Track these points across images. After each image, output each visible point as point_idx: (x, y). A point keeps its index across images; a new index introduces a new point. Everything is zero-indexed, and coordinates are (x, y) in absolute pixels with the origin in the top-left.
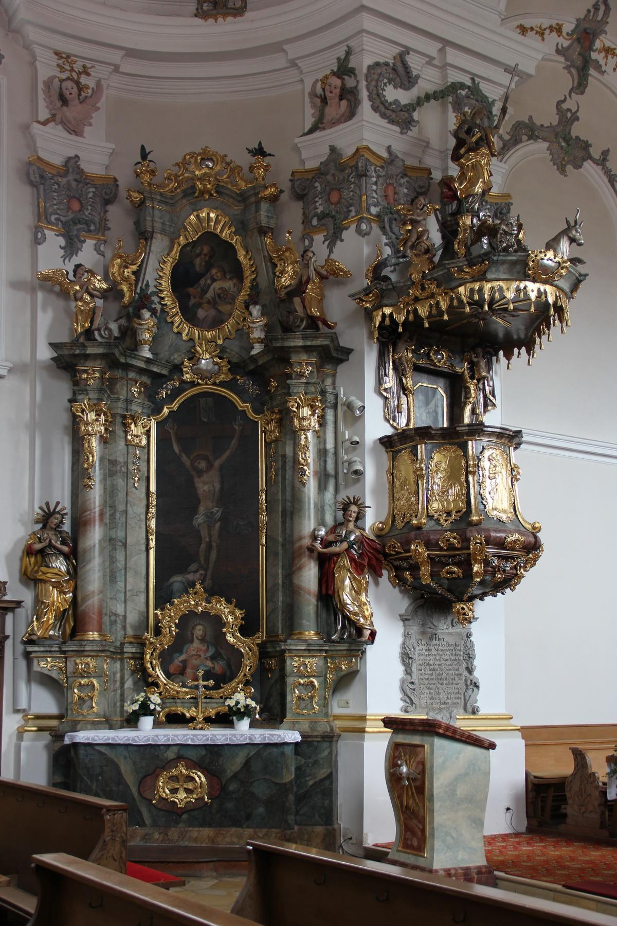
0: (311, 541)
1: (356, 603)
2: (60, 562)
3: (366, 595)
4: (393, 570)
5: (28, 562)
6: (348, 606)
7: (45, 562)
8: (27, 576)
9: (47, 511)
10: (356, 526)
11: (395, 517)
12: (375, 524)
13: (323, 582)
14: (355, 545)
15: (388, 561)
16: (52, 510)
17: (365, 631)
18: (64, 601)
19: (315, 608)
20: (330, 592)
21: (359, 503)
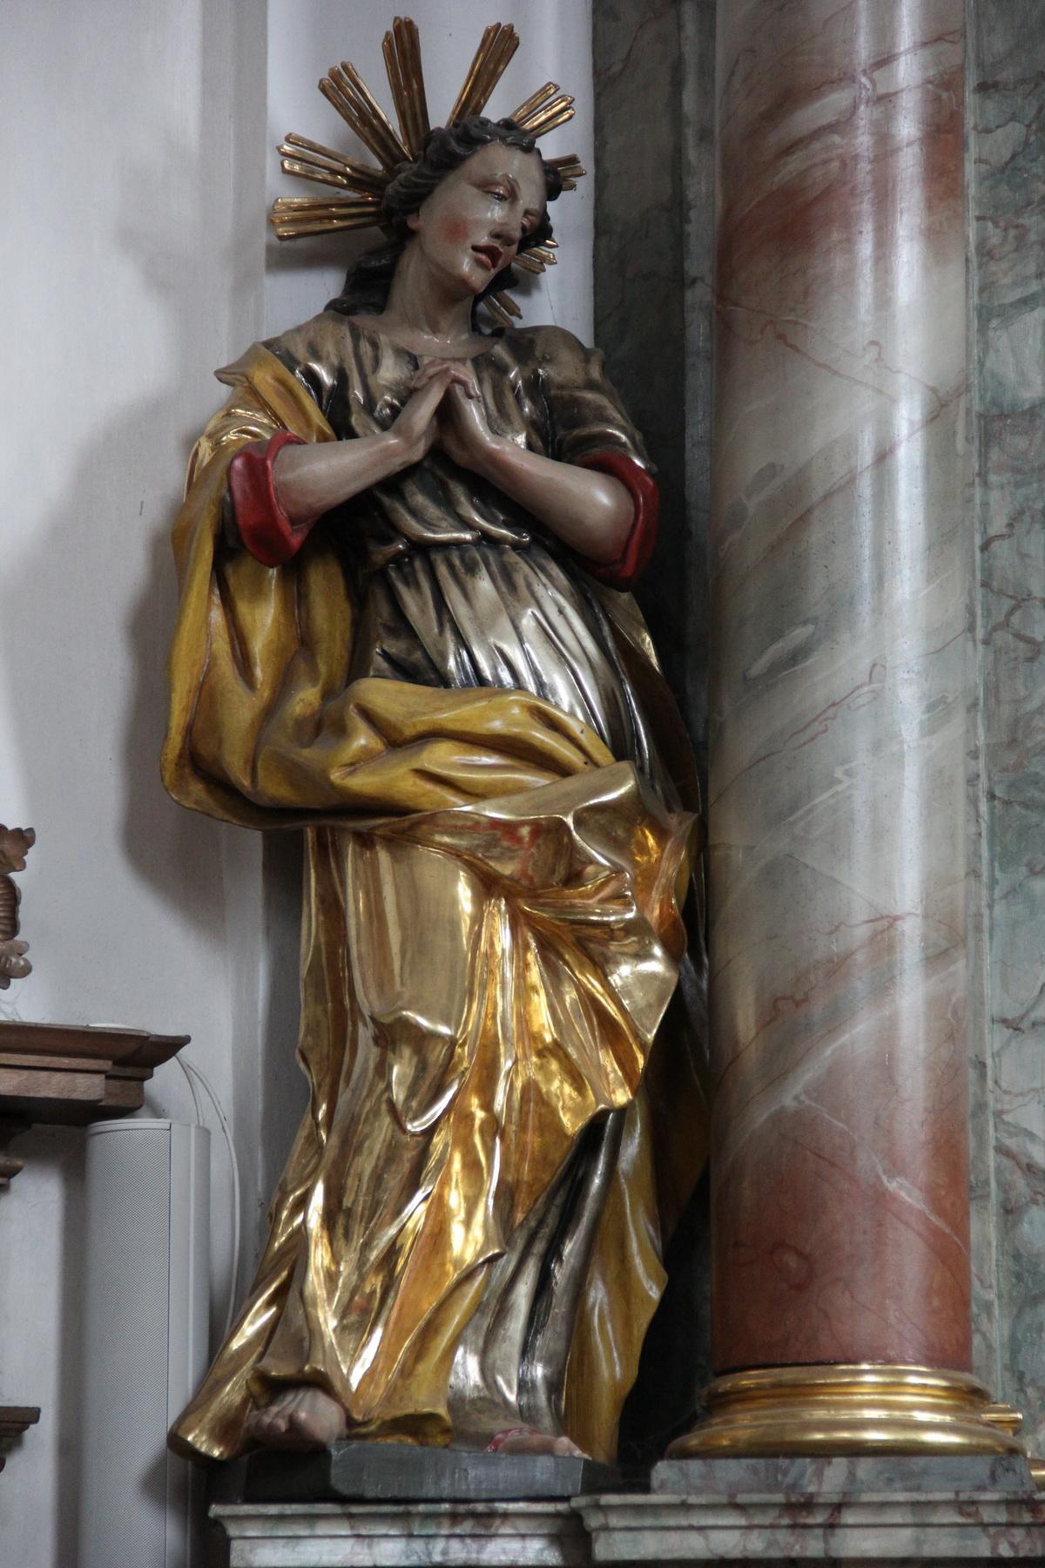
2: (549, 636)
5: (222, 646)
7: (402, 625)
8: (219, 784)
9: (388, 113)
16: (440, 114)
18: (583, 1031)
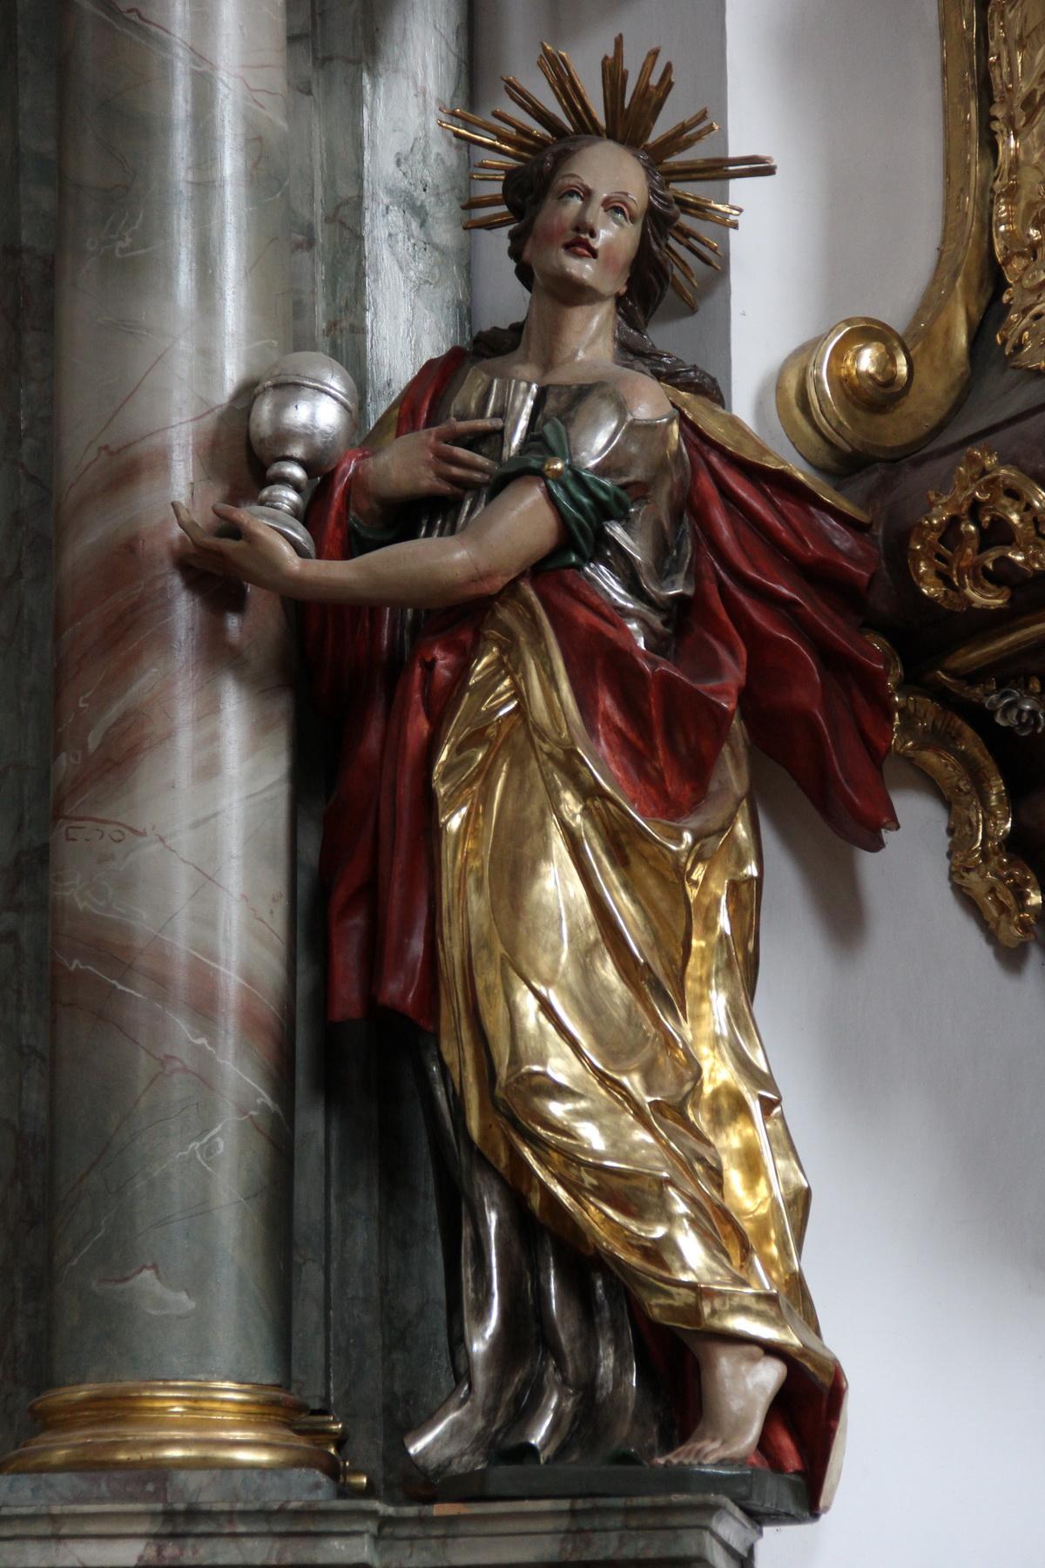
0: (215, 494)
1: (633, 1082)
3: (740, 1016)
4: (996, 788)
6: (557, 1109)
10: (632, 352)
11: (1000, 285)
12: (808, 350)
13: (341, 895)
14: (626, 521)
15: (941, 695)
17: (726, 1363)
19: (259, 1146)
20: (398, 989)
21: (660, 130)
